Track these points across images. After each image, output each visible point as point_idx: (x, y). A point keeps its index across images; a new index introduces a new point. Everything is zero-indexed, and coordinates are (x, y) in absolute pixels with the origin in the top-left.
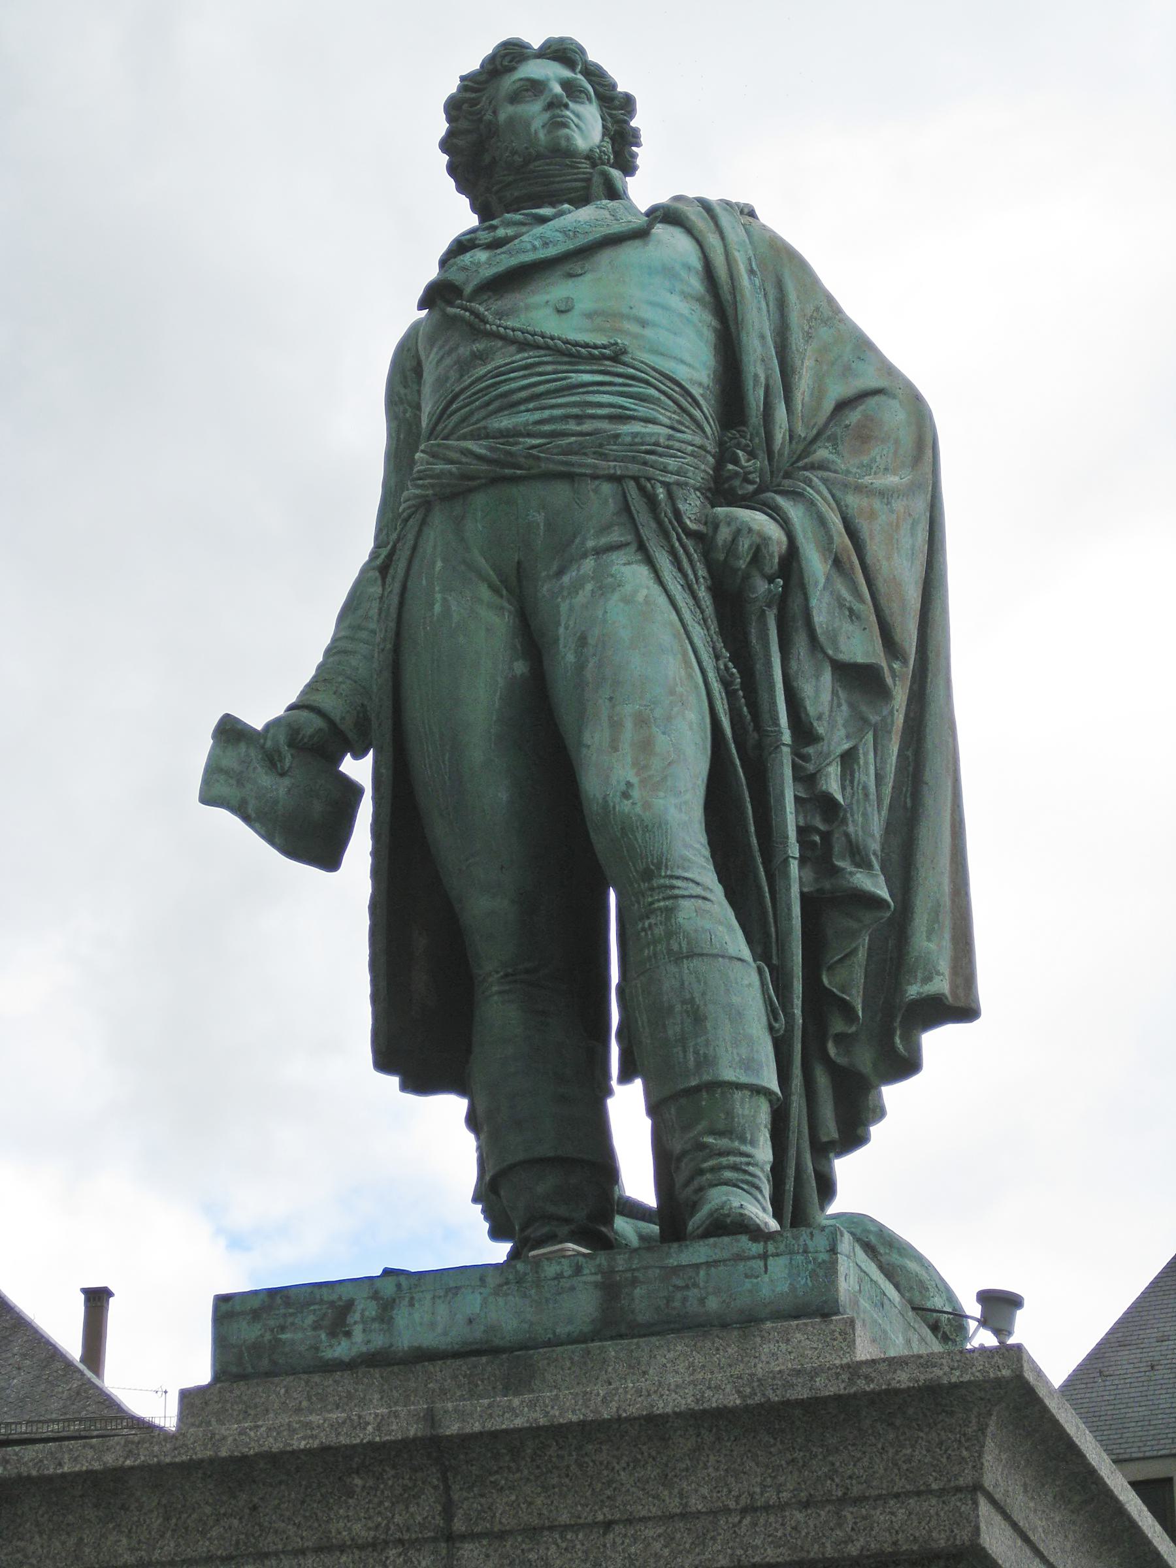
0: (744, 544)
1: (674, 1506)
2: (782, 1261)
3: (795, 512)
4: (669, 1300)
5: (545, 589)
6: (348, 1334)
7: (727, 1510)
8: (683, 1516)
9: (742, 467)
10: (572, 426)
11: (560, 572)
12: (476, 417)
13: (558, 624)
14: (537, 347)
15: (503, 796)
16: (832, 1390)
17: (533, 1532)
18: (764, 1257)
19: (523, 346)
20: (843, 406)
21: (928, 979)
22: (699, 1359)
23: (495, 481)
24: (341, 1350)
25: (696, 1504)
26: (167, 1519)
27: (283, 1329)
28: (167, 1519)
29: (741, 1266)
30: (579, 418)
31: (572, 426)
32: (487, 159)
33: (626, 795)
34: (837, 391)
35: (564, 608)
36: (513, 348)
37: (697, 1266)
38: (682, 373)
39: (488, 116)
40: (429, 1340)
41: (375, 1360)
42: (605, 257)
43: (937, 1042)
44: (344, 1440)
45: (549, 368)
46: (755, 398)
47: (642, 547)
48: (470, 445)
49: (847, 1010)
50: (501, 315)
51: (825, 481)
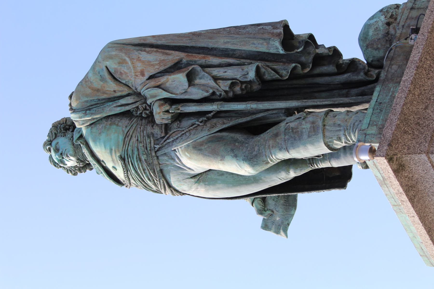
9: (143, 111)
10: (147, 171)
30: (144, 170)
38: (121, 137)
43: (298, 29)
49: (295, 68)
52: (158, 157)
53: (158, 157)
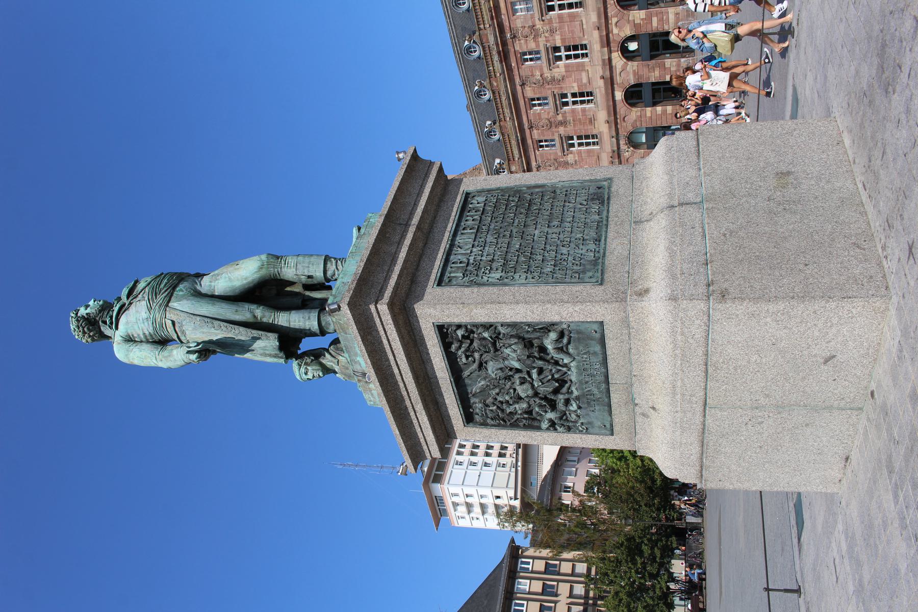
23: (174, 289)
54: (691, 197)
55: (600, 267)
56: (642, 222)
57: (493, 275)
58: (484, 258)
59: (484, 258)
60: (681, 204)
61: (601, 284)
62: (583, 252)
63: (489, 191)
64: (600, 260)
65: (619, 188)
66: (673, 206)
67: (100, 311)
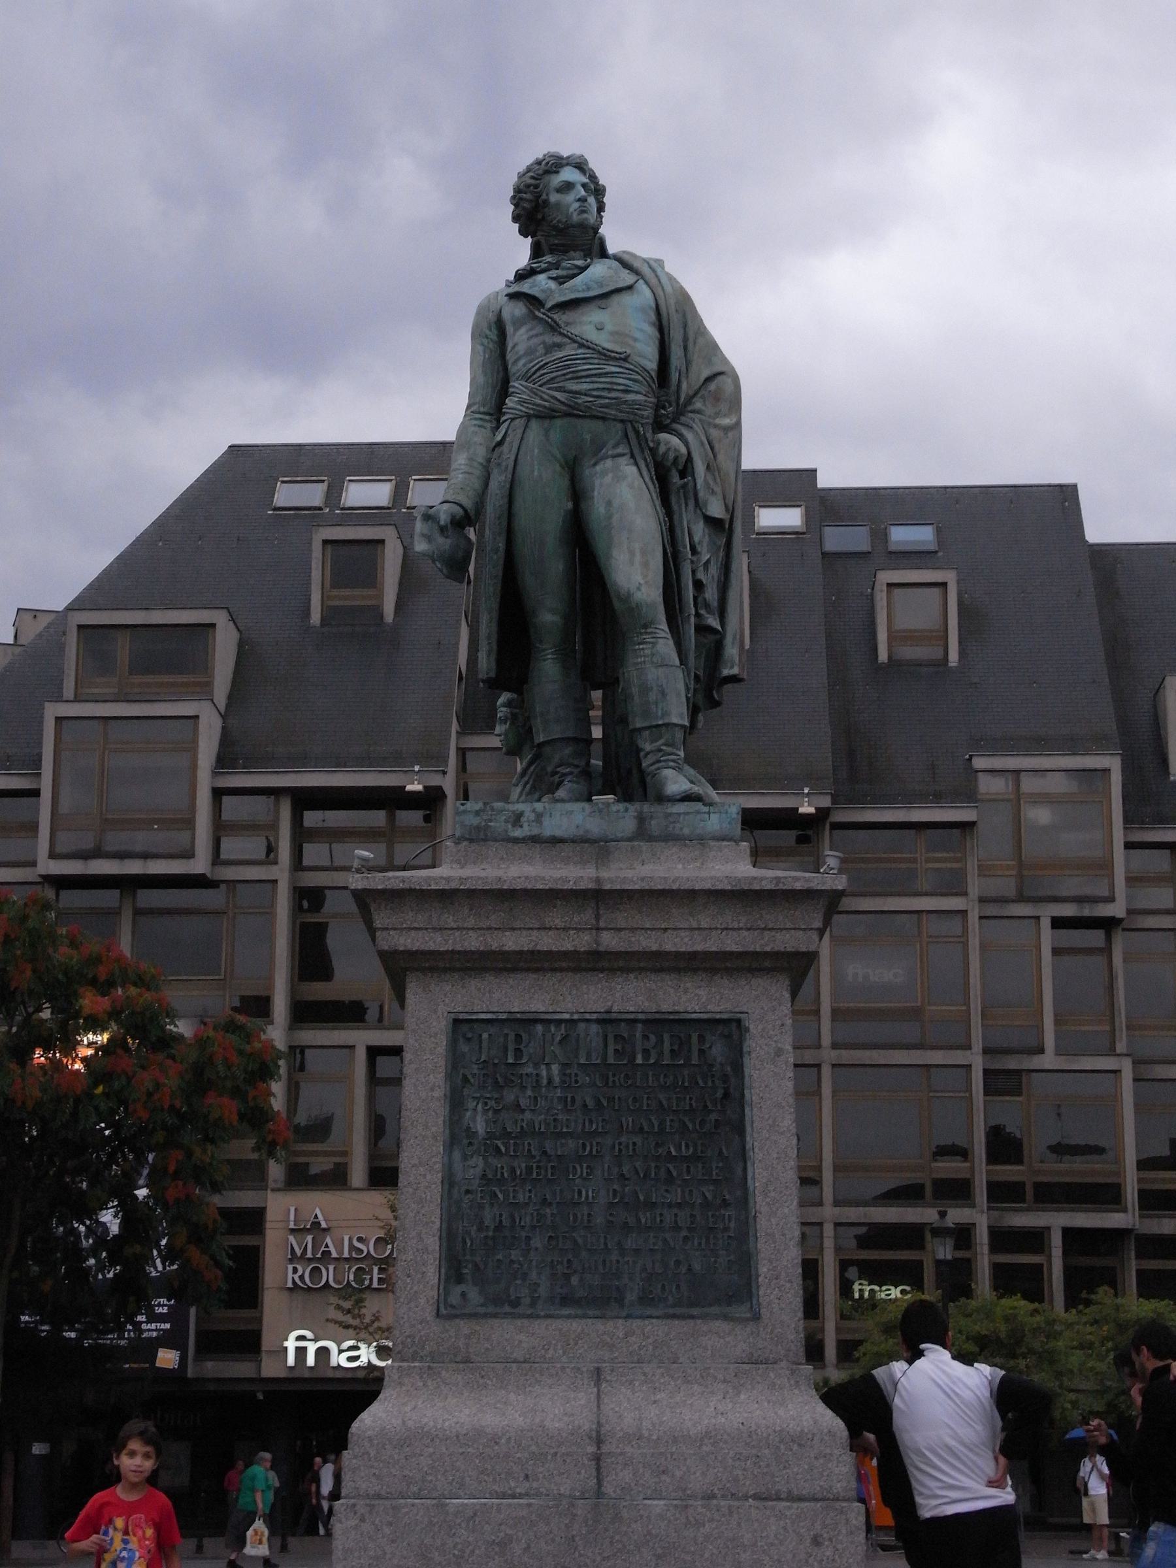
0: (671, 456)
1: (695, 925)
2: (717, 815)
3: (690, 436)
4: (667, 827)
5: (587, 472)
6: (521, 826)
7: (716, 929)
8: (699, 929)
10: (605, 394)
11: (595, 464)
12: (558, 379)
13: (593, 491)
14: (589, 348)
15: (561, 567)
16: (768, 887)
17: (633, 930)
18: (709, 813)
19: (581, 346)
20: (709, 379)
21: (732, 667)
22: (682, 855)
24: (517, 833)
25: (704, 925)
26: (471, 910)
27: (491, 821)
28: (471, 910)
29: (699, 817)
30: (610, 390)
31: (605, 394)
32: (540, 216)
33: (639, 589)
34: (706, 373)
35: (597, 483)
36: (576, 345)
37: (679, 814)
39: (544, 197)
40: (558, 833)
41: (535, 840)
42: (616, 299)
44: (559, 887)
45: (596, 361)
46: (674, 377)
47: (633, 456)
48: (558, 395)
50: (567, 324)
51: (701, 420)
52: (622, 421)
53: (622, 421)
54: (618, 1478)
55: (491, 1309)
56: (598, 1384)
57: (479, 1118)
58: (529, 1093)
59: (529, 1093)
60: (598, 1459)
61: (438, 1315)
62: (534, 1275)
63: (738, 1068)
64: (507, 1309)
65: (720, 1337)
66: (599, 1442)
67: (555, 228)
